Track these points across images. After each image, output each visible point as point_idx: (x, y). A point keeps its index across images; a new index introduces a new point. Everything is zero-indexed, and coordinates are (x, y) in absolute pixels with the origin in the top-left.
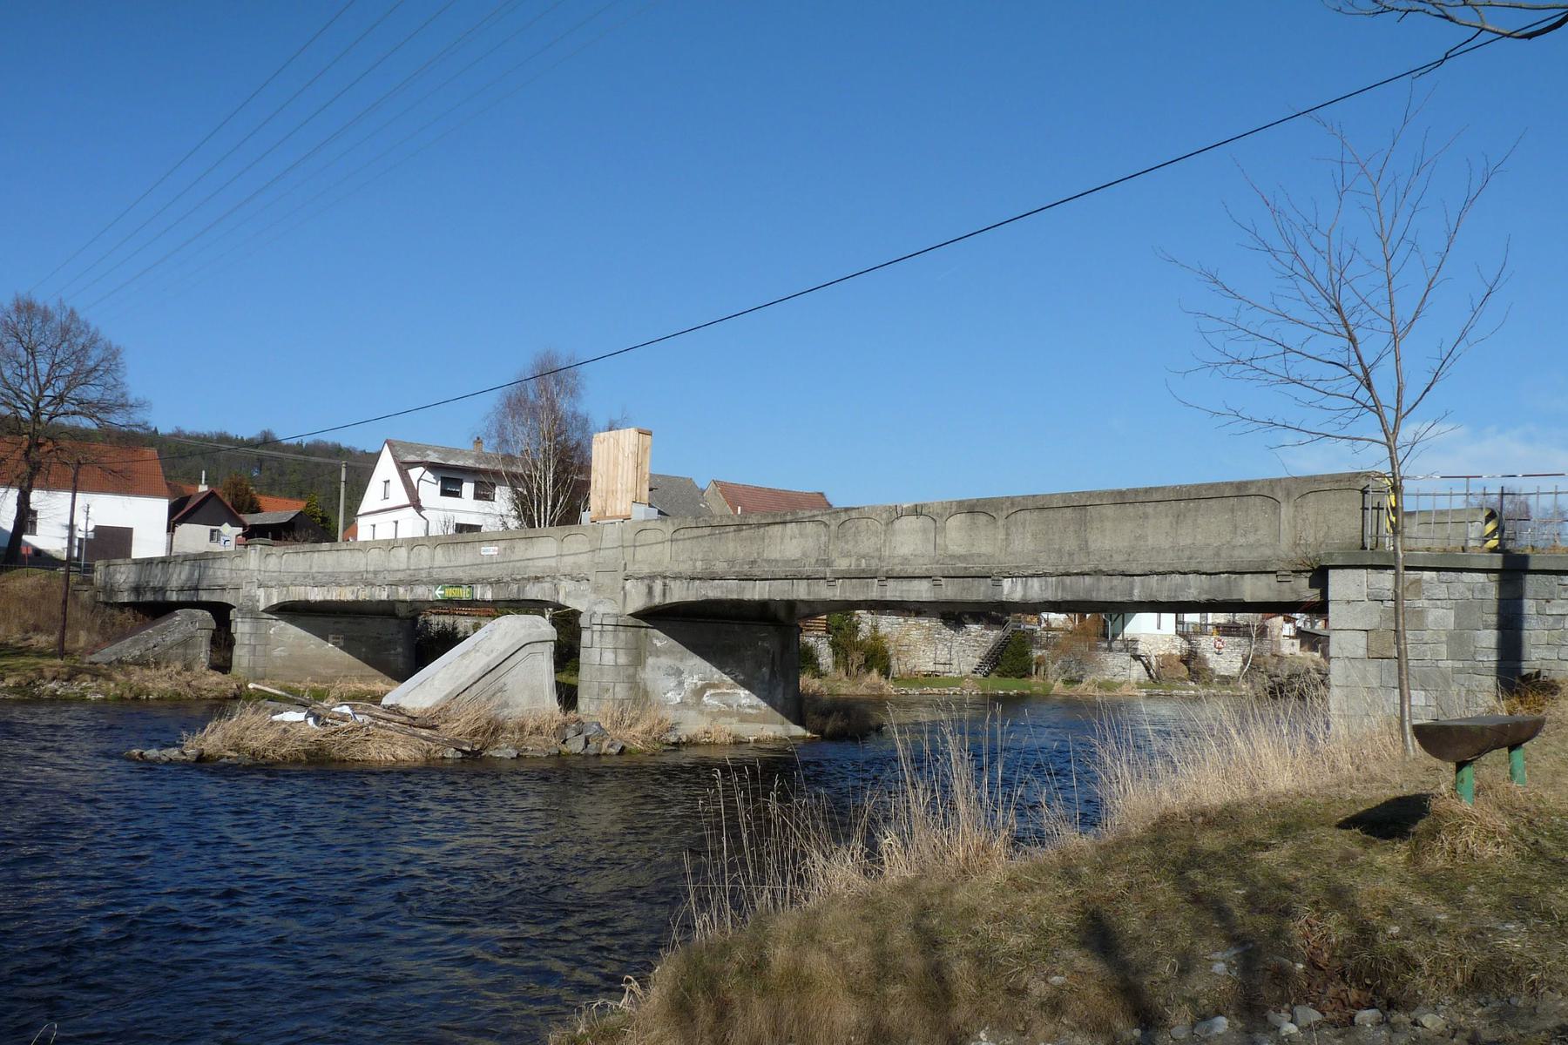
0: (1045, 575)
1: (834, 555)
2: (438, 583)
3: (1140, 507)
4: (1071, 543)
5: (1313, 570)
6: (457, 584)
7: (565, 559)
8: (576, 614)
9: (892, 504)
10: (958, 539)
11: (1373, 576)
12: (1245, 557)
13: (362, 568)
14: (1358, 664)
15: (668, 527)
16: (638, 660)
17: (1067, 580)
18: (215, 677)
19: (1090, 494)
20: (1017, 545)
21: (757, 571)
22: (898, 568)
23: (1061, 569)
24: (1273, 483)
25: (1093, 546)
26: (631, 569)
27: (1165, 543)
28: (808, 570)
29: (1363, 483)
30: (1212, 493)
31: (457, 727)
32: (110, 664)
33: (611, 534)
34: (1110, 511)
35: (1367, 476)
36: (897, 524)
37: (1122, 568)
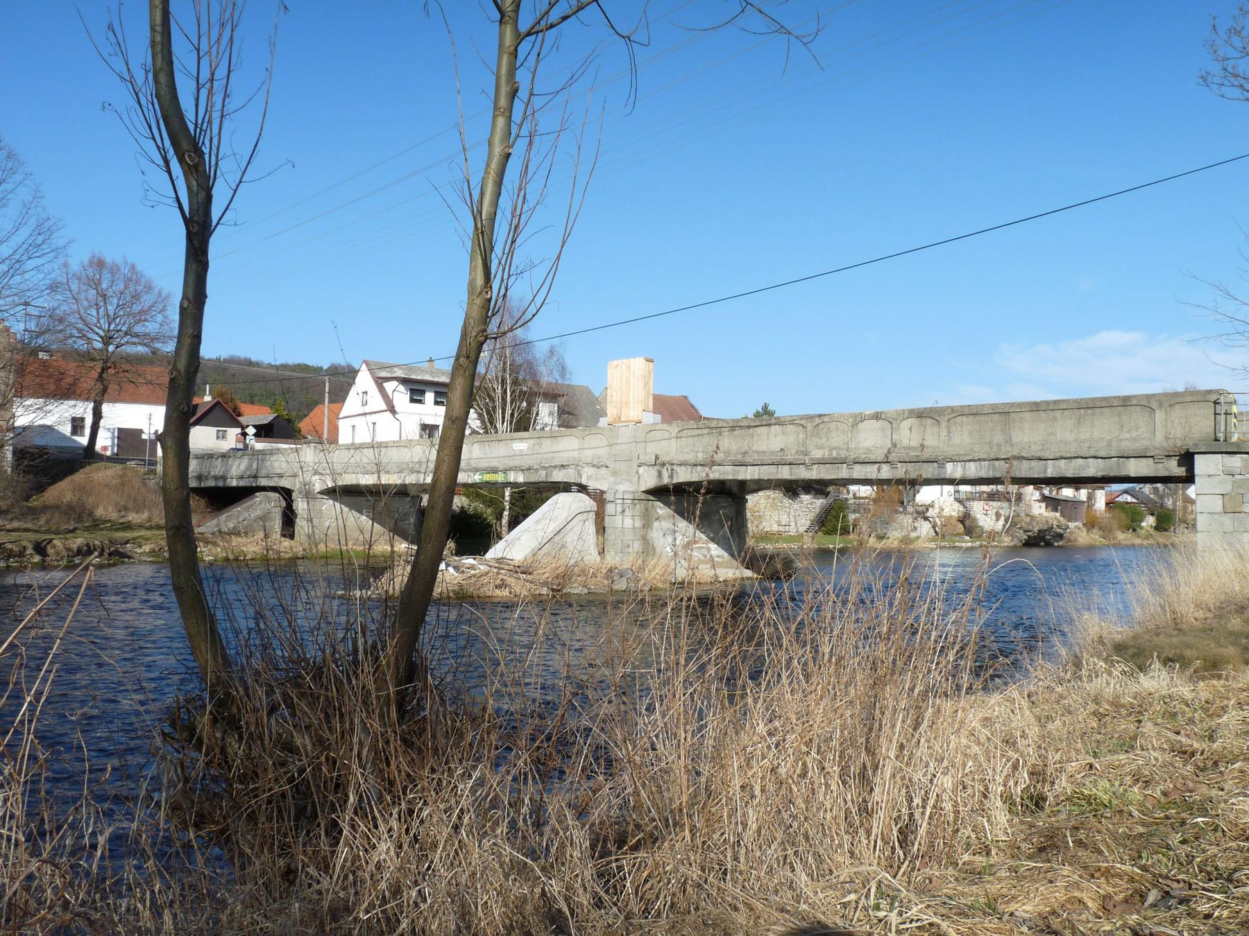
0: (980, 460)
1: (811, 448)
2: (476, 470)
3: (1051, 413)
4: (998, 438)
5: (1181, 455)
6: (494, 471)
7: (586, 452)
8: (602, 492)
9: (857, 412)
10: (908, 435)
11: (1227, 458)
12: (1128, 446)
13: (407, 459)
14: (1217, 516)
15: (674, 429)
16: (647, 526)
17: (997, 463)
18: (286, 543)
19: (1012, 405)
20: (957, 439)
21: (748, 459)
22: (863, 456)
23: (992, 456)
24: (1149, 397)
25: (1015, 440)
26: (643, 459)
27: (1069, 437)
28: (790, 458)
29: (1214, 397)
30: (1104, 404)
31: (545, 574)
32: (213, 534)
33: (625, 434)
34: (1027, 416)
35: (1217, 391)
36: (861, 426)
37: (1038, 454)
